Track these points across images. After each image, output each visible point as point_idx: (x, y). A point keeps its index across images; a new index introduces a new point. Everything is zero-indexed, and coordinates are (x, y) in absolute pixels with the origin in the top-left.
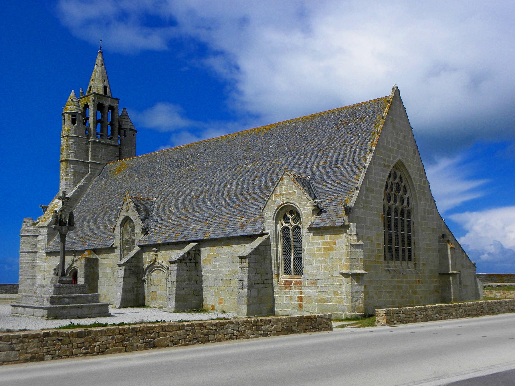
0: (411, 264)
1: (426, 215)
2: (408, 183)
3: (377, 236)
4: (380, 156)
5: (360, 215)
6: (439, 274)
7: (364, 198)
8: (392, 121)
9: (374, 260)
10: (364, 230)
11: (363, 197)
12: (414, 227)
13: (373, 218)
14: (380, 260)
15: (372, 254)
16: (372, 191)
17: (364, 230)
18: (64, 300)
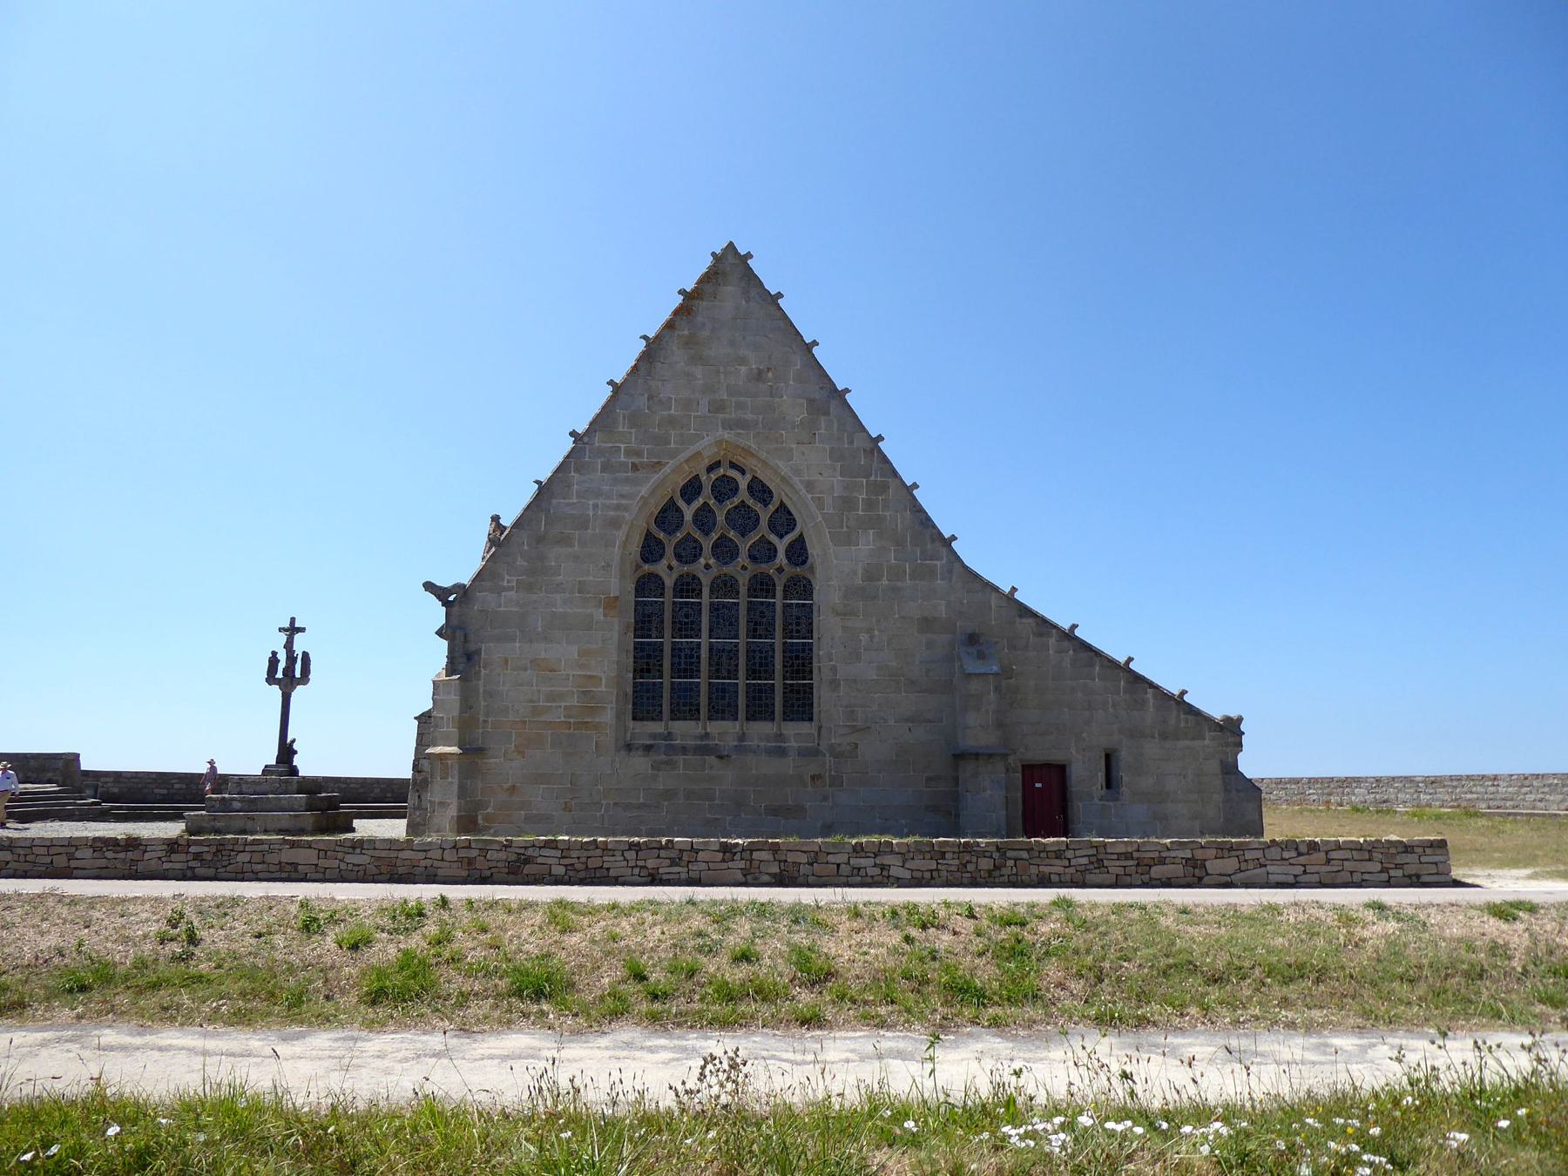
0: (796, 732)
1: (885, 582)
2: (791, 499)
3: (578, 655)
4: (610, 445)
5: (500, 606)
6: (954, 755)
7: (520, 562)
8: (690, 342)
9: (563, 719)
10: (518, 645)
11: (519, 559)
12: (819, 620)
13: (561, 610)
14: (589, 720)
15: (549, 704)
16: (565, 541)
17: (518, 645)
18: (231, 804)
